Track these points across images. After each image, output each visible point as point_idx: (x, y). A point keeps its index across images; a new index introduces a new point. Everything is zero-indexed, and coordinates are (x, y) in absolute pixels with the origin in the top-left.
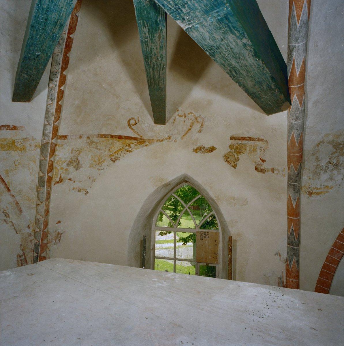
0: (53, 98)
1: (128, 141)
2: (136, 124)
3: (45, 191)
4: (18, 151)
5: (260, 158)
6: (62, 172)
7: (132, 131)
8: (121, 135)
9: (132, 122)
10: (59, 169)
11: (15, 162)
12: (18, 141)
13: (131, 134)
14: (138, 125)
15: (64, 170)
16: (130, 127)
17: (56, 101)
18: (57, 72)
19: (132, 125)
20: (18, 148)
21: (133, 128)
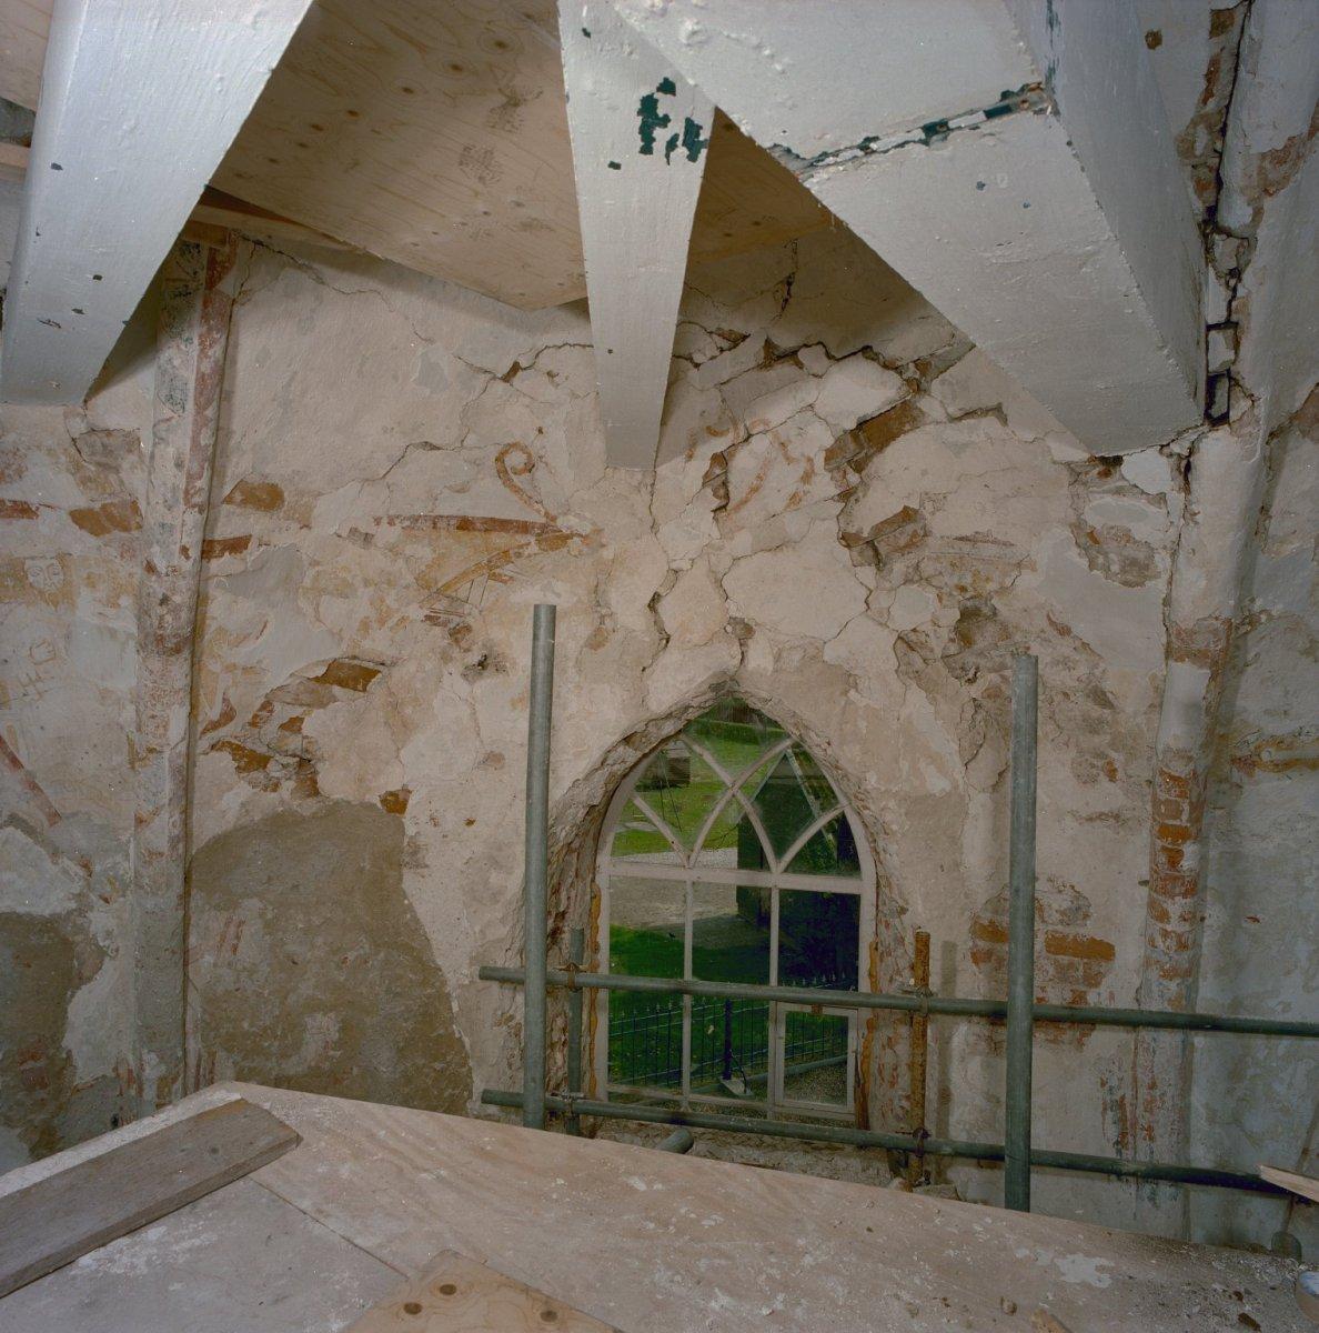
0: (178, 395)
1: (500, 540)
2: (530, 468)
3: (167, 769)
4: (44, 605)
5: (1048, 616)
6: (230, 683)
7: (515, 497)
8: (470, 513)
9: (516, 459)
10: (219, 671)
11: (31, 649)
12: (37, 562)
13: (512, 510)
14: (540, 473)
15: (239, 672)
16: (508, 482)
17: (190, 406)
18: (193, 285)
19: (515, 474)
20: (41, 592)
21: (519, 484)
